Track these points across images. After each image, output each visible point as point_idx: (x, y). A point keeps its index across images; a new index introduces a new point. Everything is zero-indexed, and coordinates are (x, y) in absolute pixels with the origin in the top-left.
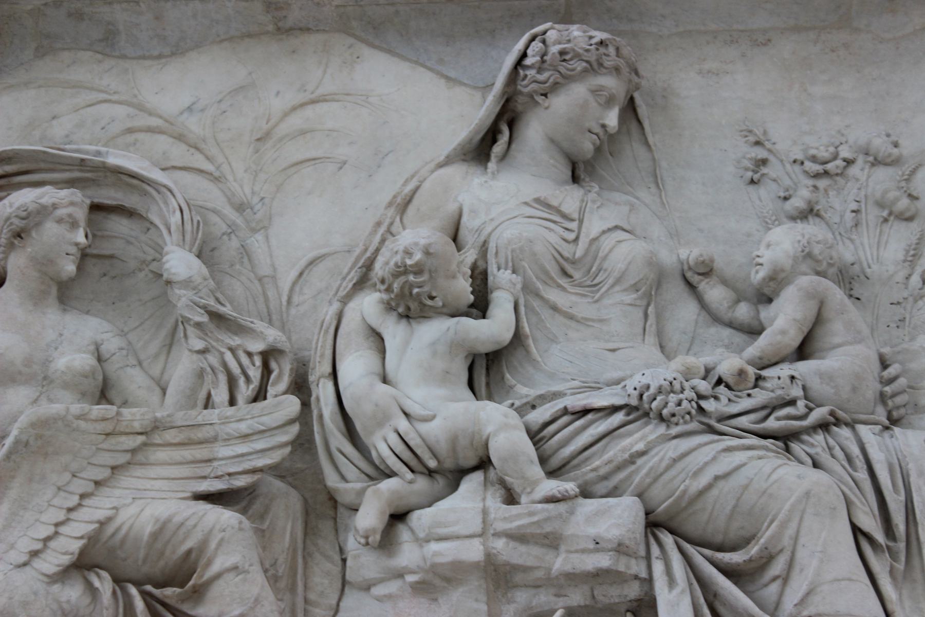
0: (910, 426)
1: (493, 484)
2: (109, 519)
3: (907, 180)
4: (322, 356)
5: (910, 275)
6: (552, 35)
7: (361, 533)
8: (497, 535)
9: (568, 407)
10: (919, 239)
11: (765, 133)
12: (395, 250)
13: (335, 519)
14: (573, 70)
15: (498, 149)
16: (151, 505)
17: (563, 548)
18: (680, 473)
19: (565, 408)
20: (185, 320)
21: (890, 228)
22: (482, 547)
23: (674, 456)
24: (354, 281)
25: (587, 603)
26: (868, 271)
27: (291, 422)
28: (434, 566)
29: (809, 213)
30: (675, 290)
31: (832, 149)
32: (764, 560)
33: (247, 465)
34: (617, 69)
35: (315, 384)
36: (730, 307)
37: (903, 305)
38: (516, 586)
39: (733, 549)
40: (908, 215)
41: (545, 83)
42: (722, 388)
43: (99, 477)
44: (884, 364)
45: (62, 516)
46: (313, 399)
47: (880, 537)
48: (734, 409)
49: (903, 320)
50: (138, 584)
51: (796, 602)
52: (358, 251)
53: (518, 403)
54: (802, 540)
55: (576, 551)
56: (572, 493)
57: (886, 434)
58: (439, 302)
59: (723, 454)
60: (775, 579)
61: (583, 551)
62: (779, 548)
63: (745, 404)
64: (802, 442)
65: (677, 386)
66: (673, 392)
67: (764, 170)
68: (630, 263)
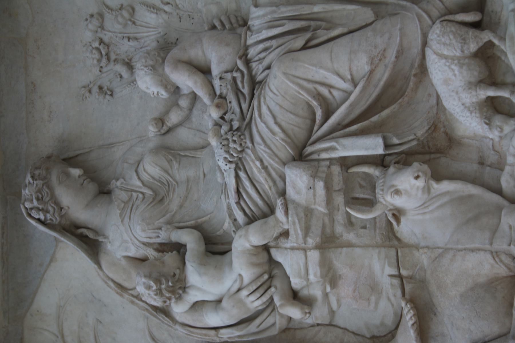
0: (248, 14)
1: (278, 244)
3: (112, 10)
4: (206, 335)
5: (165, 11)
6: (28, 205)
7: (303, 316)
8: (305, 242)
9: (236, 201)
10: (145, 5)
11: (84, 87)
12: (147, 295)
13: (295, 329)
14: (47, 193)
15: (91, 235)
17: (313, 207)
18: (273, 142)
19: (236, 203)
21: (138, 20)
22: (312, 251)
23: (263, 145)
24: (164, 316)
25: (342, 193)
26: (162, 34)
28: (322, 277)
29: (129, 66)
31: (94, 51)
32: (320, 98)
34: (47, 169)
35: (221, 339)
36: (181, 110)
37: (181, 15)
38: (333, 232)
39: (314, 114)
40: (131, 11)
41: (54, 209)
42: (226, 117)
44: (214, 27)
46: (229, 340)
47: (308, 35)
48: (237, 110)
51: (343, 82)
52: (147, 314)
53: (234, 229)
54: (310, 77)
55: (315, 199)
56: (283, 201)
58: (177, 272)
59: (263, 118)
60: (330, 92)
61: (314, 195)
62: (314, 90)
63: (234, 104)
64: (256, 74)
65: (225, 143)
66: (228, 145)
67: (105, 88)
68: (156, 164)
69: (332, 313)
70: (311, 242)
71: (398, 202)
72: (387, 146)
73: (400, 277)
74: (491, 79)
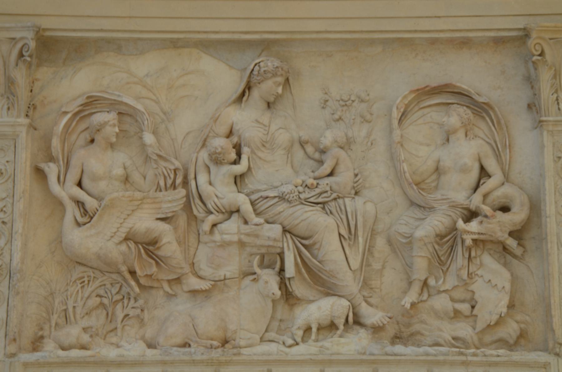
2: (132, 227)
6: (262, 64)
8: (242, 234)
15: (245, 98)
16: (144, 222)
20: (150, 157)
27: (183, 197)
30: (297, 146)
31: (349, 97)
33: (171, 210)
34: (282, 75)
43: (129, 213)
44: (356, 175)
45: (119, 225)
49: (364, 157)
50: (141, 244)
57: (353, 201)
58: (226, 161)
63: (313, 193)
65: (293, 191)
66: (291, 193)
67: (328, 103)
69: (206, 243)
70: (242, 237)
71: (261, 282)
72: (289, 279)
73: (225, 279)
74: (320, 328)
